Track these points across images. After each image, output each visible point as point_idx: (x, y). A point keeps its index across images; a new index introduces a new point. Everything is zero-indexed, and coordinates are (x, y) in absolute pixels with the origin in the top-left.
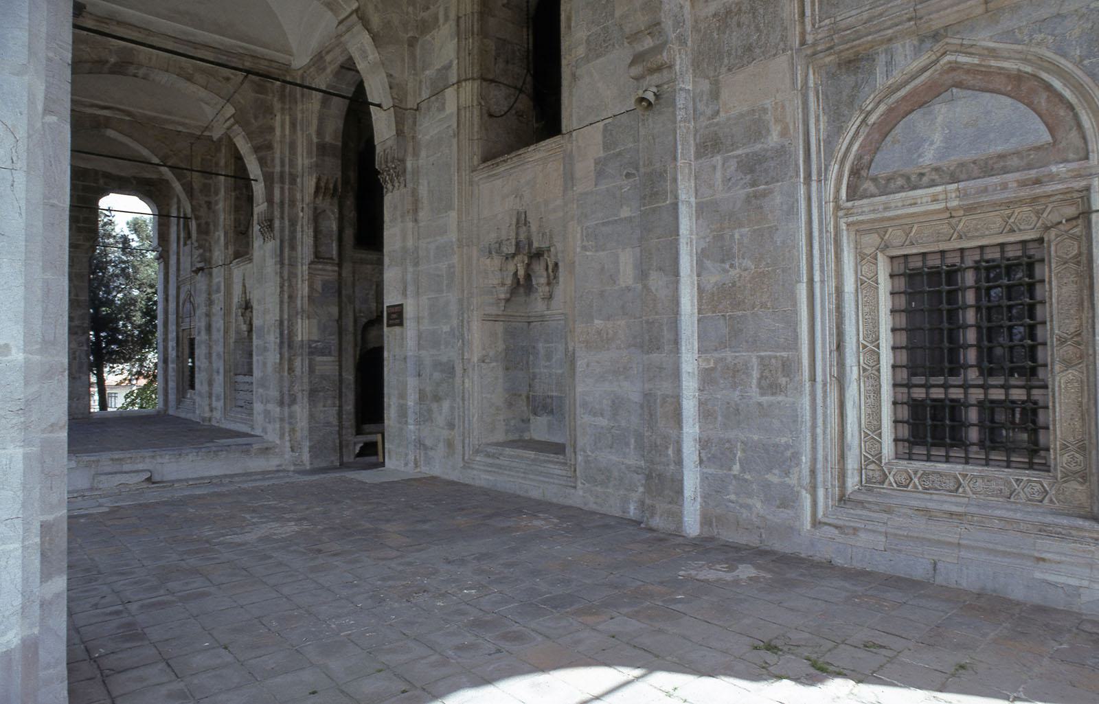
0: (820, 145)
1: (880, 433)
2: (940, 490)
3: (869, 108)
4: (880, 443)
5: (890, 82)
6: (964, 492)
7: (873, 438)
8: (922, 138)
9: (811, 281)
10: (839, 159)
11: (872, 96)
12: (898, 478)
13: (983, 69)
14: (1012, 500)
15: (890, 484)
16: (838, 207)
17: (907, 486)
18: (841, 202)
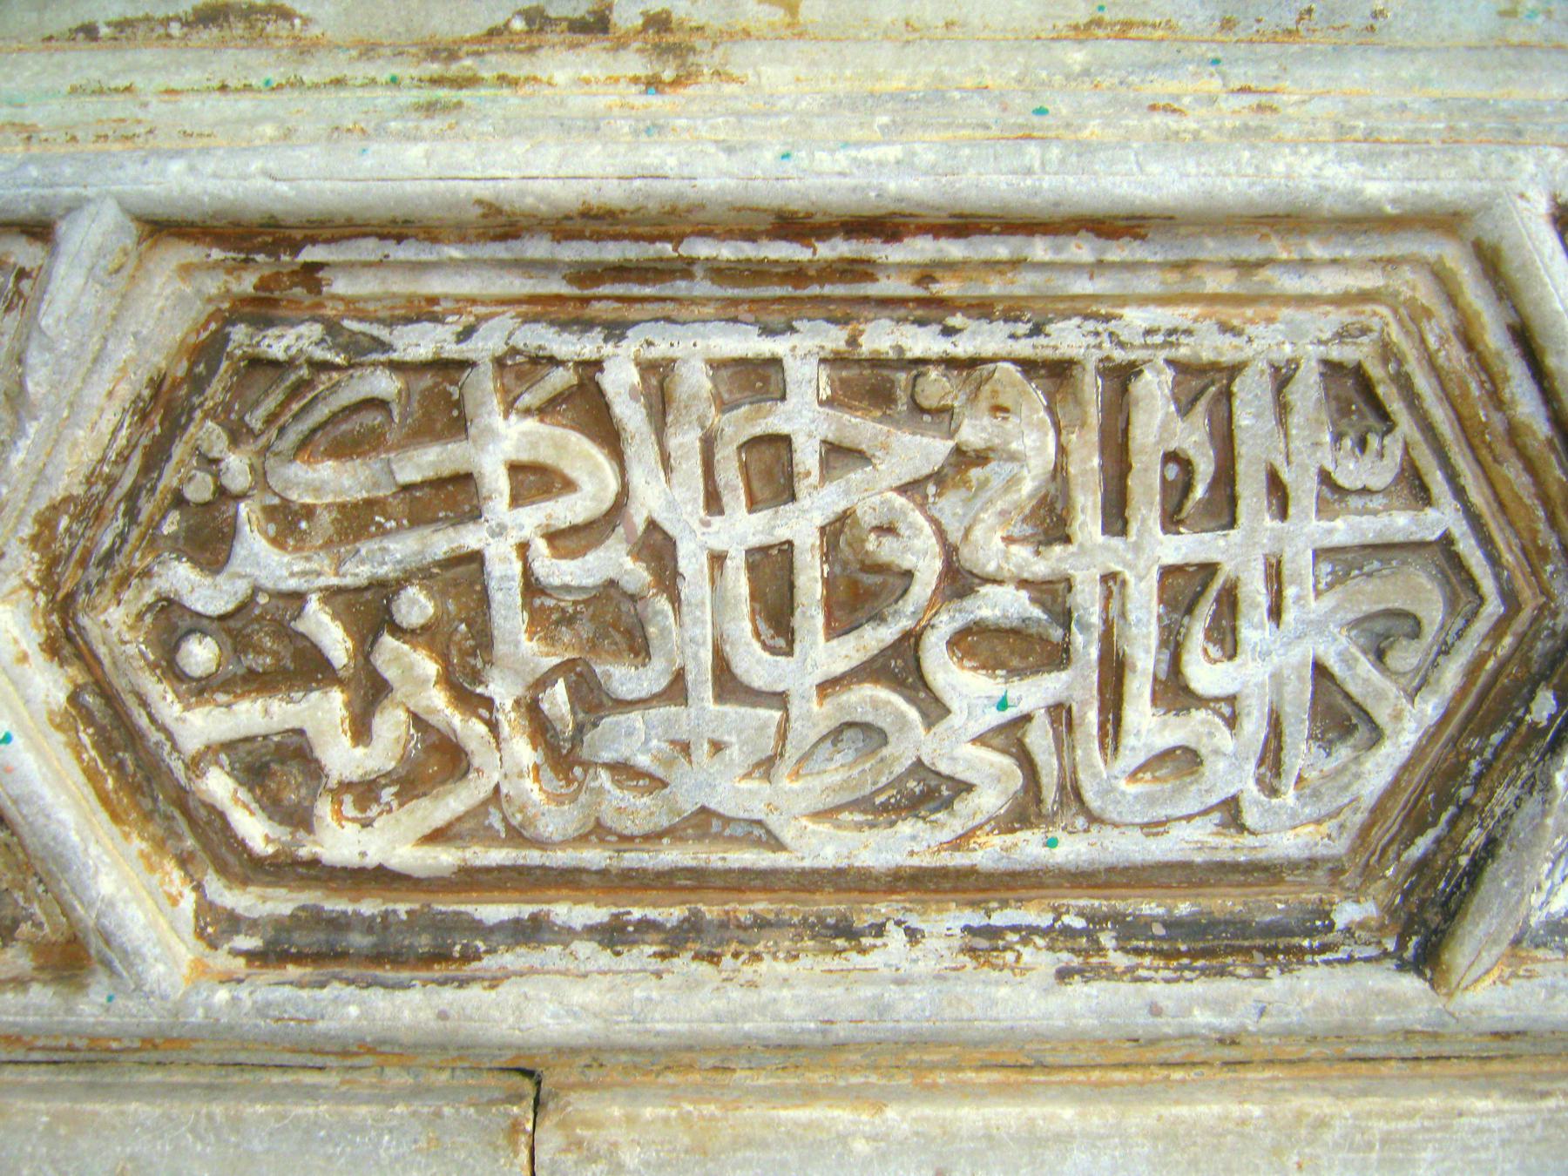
2: (835, 911)
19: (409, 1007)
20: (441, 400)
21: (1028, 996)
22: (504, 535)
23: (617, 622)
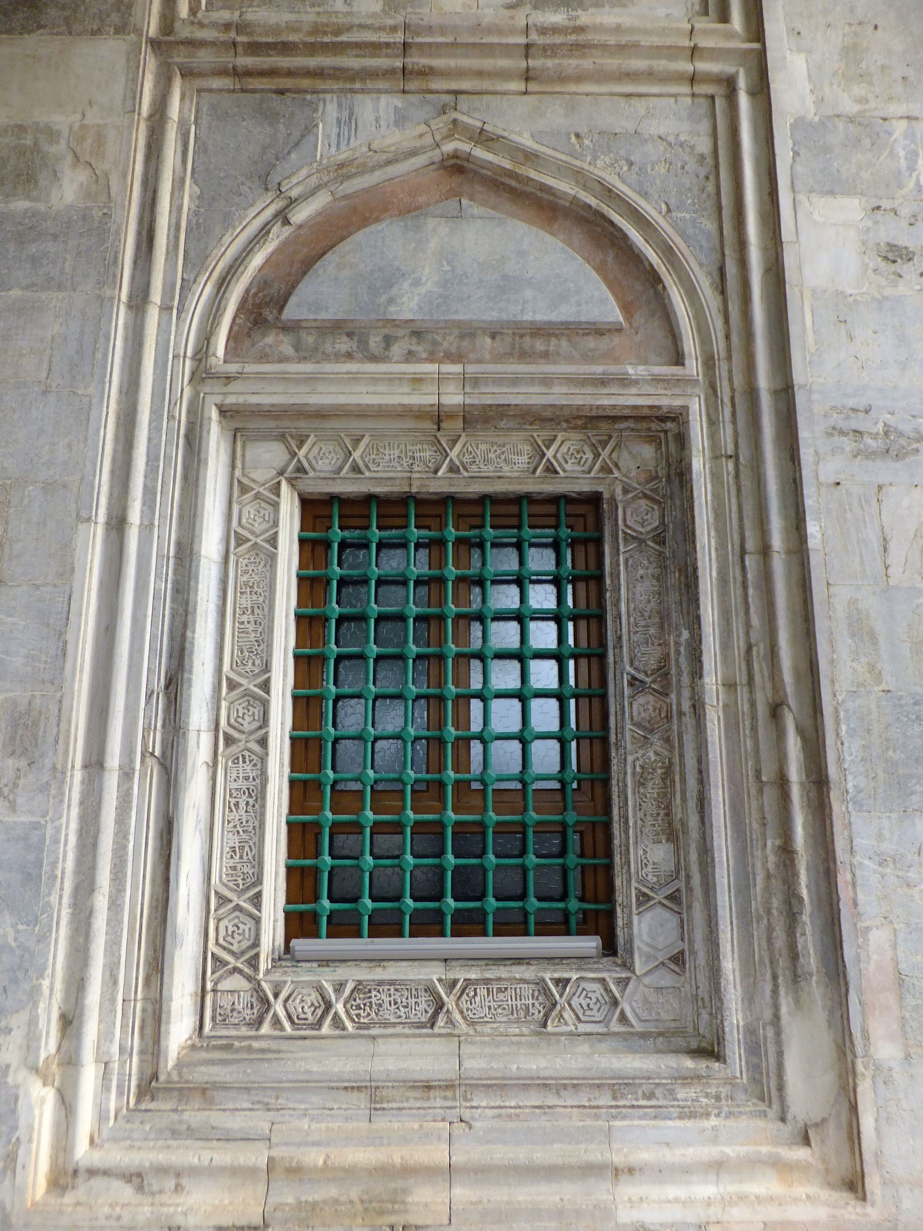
0: (177, 238)
1: (259, 895)
2: (394, 1025)
3: (294, 193)
4: (257, 921)
5: (342, 157)
6: (450, 1022)
7: (238, 908)
8: (398, 269)
9: (117, 524)
10: (216, 275)
11: (304, 172)
12: (295, 1006)
13: (513, 183)
14: (550, 1028)
15: (277, 1022)
16: (202, 374)
17: (319, 1024)
18: (212, 361)
19: (366, 1032)
20: (370, 991)
21: (407, 1031)
22: (373, 1000)
23: (380, 1005)
